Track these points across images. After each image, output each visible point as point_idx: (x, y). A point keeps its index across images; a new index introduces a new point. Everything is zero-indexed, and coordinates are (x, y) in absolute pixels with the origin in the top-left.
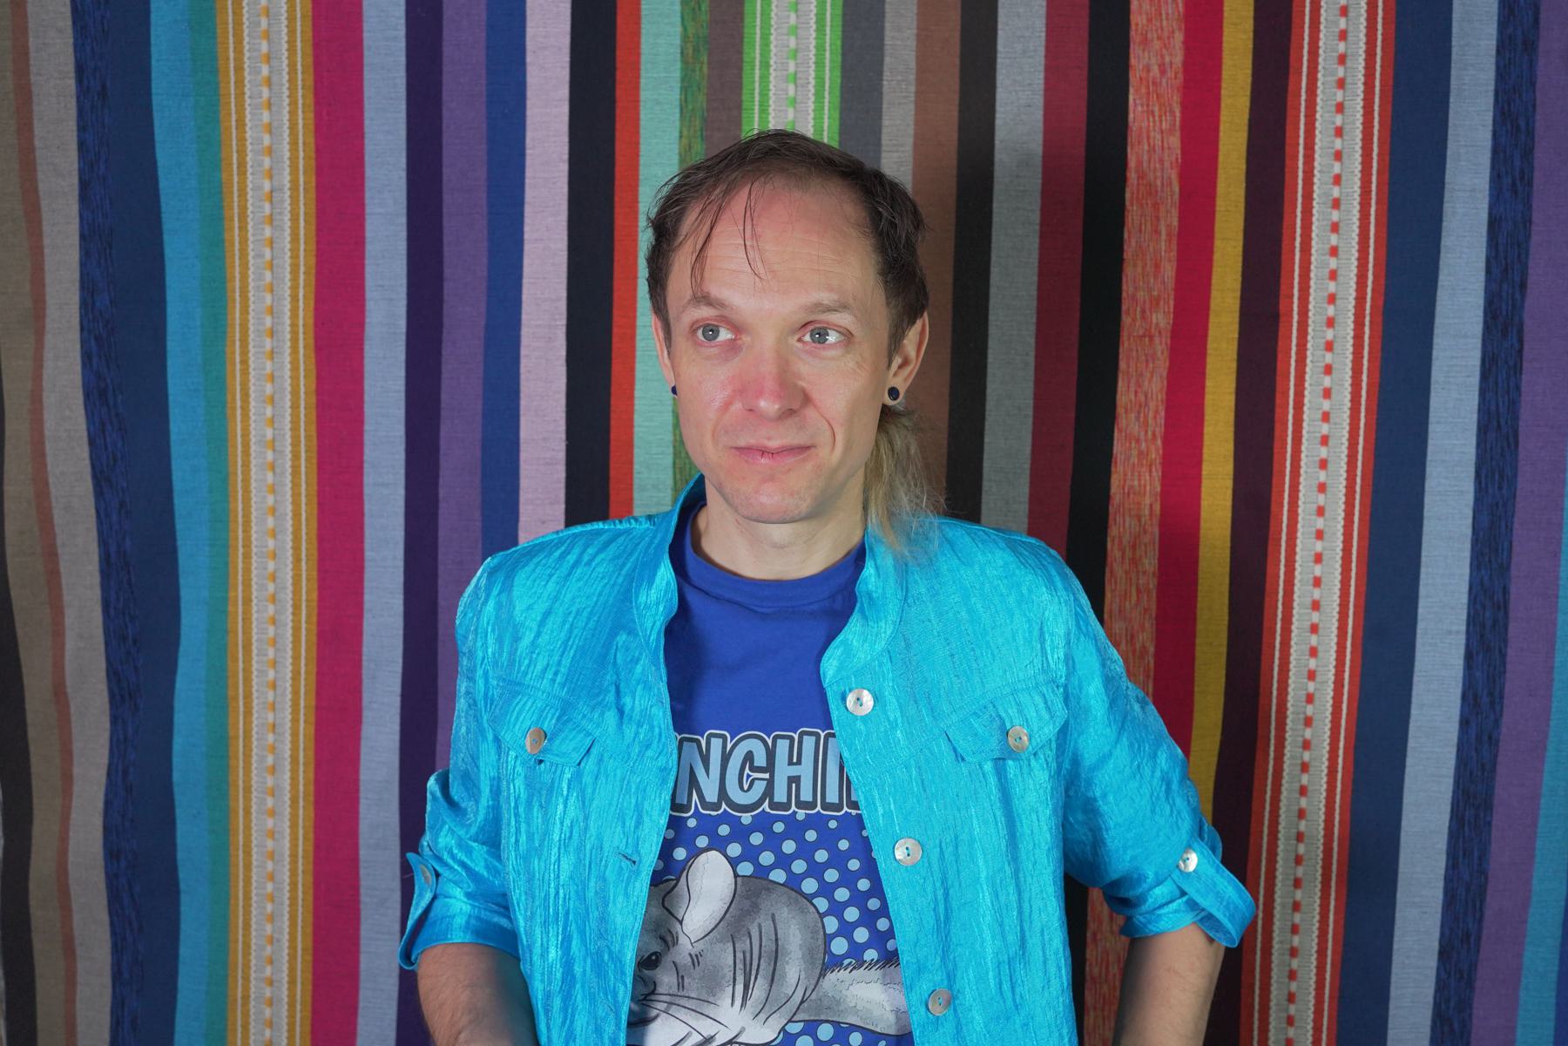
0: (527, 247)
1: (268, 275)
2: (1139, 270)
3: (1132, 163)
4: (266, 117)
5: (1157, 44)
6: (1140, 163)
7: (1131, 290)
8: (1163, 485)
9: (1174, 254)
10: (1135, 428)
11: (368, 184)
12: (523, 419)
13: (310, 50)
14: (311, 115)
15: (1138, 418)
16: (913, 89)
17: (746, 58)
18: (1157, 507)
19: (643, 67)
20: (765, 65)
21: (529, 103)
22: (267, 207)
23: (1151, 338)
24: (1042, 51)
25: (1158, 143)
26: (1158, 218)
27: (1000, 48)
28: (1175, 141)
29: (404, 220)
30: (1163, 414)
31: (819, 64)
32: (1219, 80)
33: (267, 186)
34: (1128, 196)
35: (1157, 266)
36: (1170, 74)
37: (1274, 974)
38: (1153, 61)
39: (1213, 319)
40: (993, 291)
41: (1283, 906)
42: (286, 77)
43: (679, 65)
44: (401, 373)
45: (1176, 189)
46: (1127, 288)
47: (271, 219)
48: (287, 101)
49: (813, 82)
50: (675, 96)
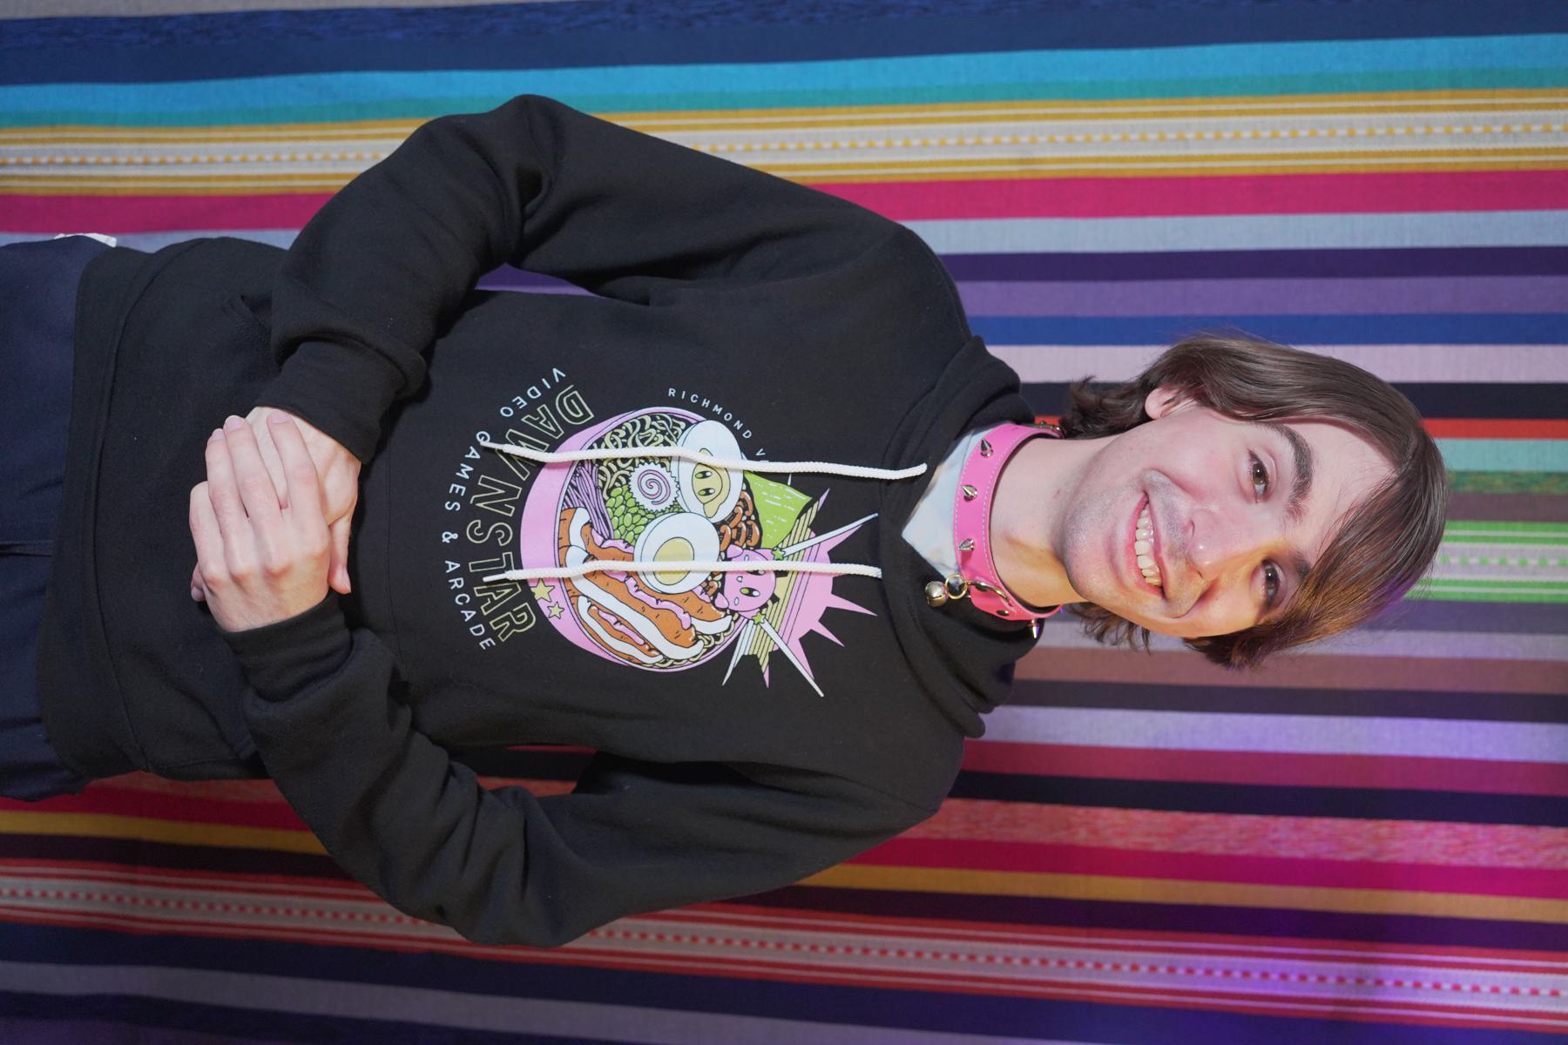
1: (1116, 137)
4: (1247, 134)
5: (1295, 837)
9: (1131, 847)
13: (1300, 171)
14: (1246, 172)
22: (1172, 136)
28: (1219, 850)
33: (1190, 136)
42: (1278, 150)
45: (1183, 850)
46: (1105, 812)
47: (1162, 139)
48: (1259, 151)
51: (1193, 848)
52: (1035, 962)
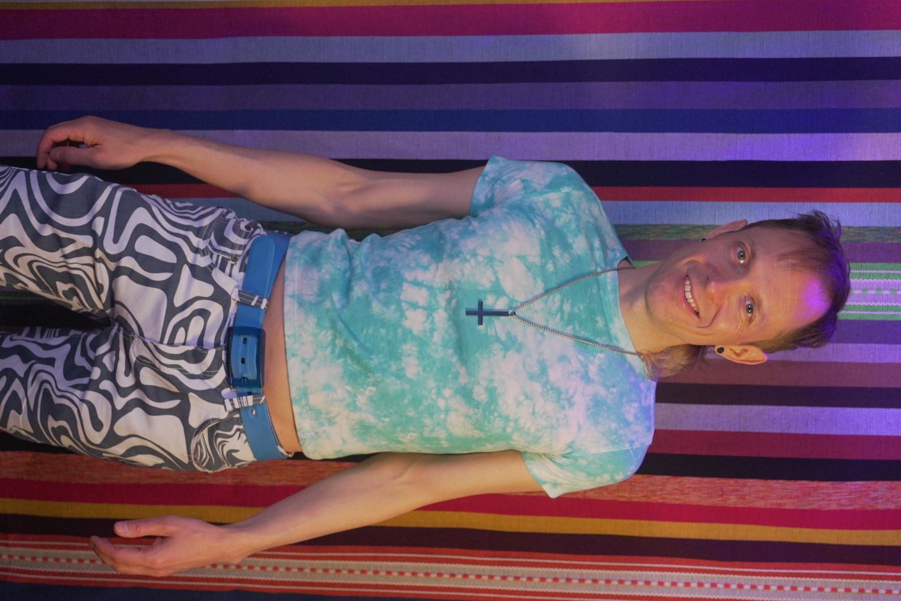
0: (785, 136)
2: (761, 489)
3: (822, 484)
6: (822, 488)
7: (749, 484)
8: (635, 503)
9: (769, 506)
10: (669, 488)
11: (827, 33)
12: (679, 134)
15: (675, 489)
16: (870, 361)
17: (892, 265)
18: (623, 499)
19: (892, 204)
20: (888, 276)
21: (874, 135)
23: (722, 495)
24: (889, 434)
25: (833, 498)
26: (791, 498)
27: (891, 410)
28: (834, 507)
29: (804, 55)
30: (677, 502)
31: (887, 308)
32: (867, 529)
34: (804, 482)
35: (763, 498)
36: (872, 503)
37: (363, 563)
38: (880, 493)
39: (730, 526)
40: (749, 407)
41: (402, 567)
43: (893, 225)
44: (708, 55)
45: (806, 508)
46: (750, 482)
49: (876, 304)
50: (875, 223)
51: (815, 506)
52: (694, 585)
